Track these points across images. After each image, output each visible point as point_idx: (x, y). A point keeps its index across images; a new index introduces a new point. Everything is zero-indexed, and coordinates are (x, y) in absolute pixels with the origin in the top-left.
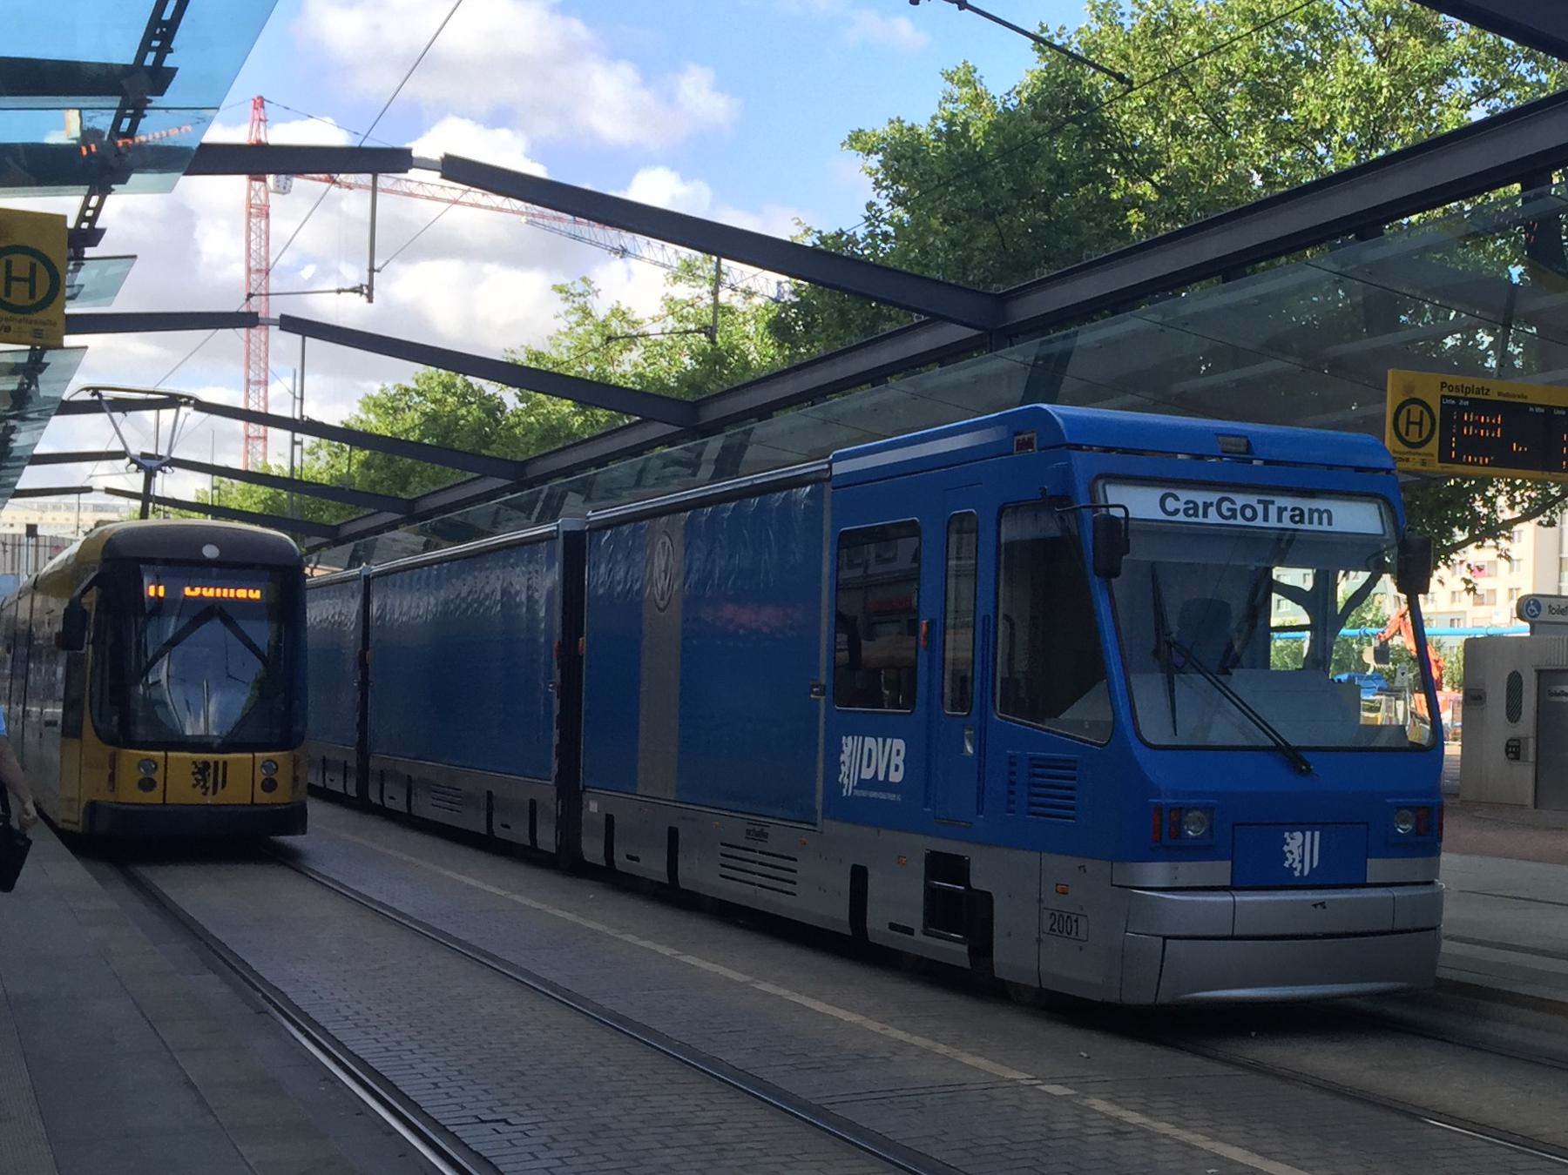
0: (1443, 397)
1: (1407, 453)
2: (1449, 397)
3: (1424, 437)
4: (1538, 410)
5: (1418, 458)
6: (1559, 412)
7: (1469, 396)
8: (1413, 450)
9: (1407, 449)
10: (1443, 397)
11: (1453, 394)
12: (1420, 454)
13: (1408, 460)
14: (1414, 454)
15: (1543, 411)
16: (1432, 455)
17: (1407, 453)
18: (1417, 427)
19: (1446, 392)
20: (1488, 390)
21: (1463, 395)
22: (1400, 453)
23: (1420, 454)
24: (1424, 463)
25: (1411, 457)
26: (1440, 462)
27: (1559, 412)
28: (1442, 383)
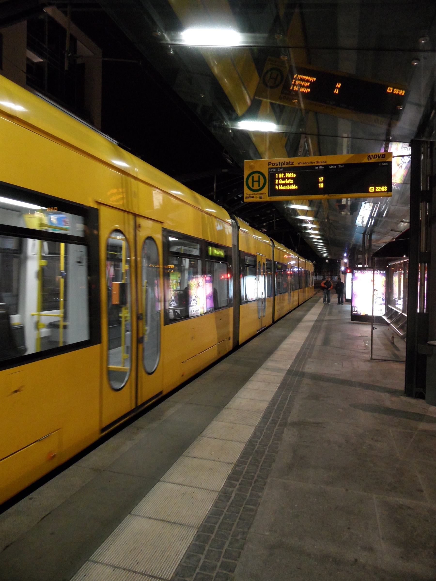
0: (269, 168)
1: (253, 194)
2: (272, 168)
3: (261, 186)
4: (320, 167)
5: (258, 196)
6: (332, 167)
7: (282, 166)
8: (255, 193)
9: (252, 193)
10: (269, 168)
11: (275, 166)
12: (259, 194)
13: (253, 197)
15: (323, 167)
16: (265, 194)
17: (253, 194)
18: (257, 183)
19: (271, 166)
20: (293, 162)
21: (280, 166)
22: (250, 194)
23: (259, 194)
24: (261, 197)
25: (255, 196)
26: (269, 196)
27: (332, 167)
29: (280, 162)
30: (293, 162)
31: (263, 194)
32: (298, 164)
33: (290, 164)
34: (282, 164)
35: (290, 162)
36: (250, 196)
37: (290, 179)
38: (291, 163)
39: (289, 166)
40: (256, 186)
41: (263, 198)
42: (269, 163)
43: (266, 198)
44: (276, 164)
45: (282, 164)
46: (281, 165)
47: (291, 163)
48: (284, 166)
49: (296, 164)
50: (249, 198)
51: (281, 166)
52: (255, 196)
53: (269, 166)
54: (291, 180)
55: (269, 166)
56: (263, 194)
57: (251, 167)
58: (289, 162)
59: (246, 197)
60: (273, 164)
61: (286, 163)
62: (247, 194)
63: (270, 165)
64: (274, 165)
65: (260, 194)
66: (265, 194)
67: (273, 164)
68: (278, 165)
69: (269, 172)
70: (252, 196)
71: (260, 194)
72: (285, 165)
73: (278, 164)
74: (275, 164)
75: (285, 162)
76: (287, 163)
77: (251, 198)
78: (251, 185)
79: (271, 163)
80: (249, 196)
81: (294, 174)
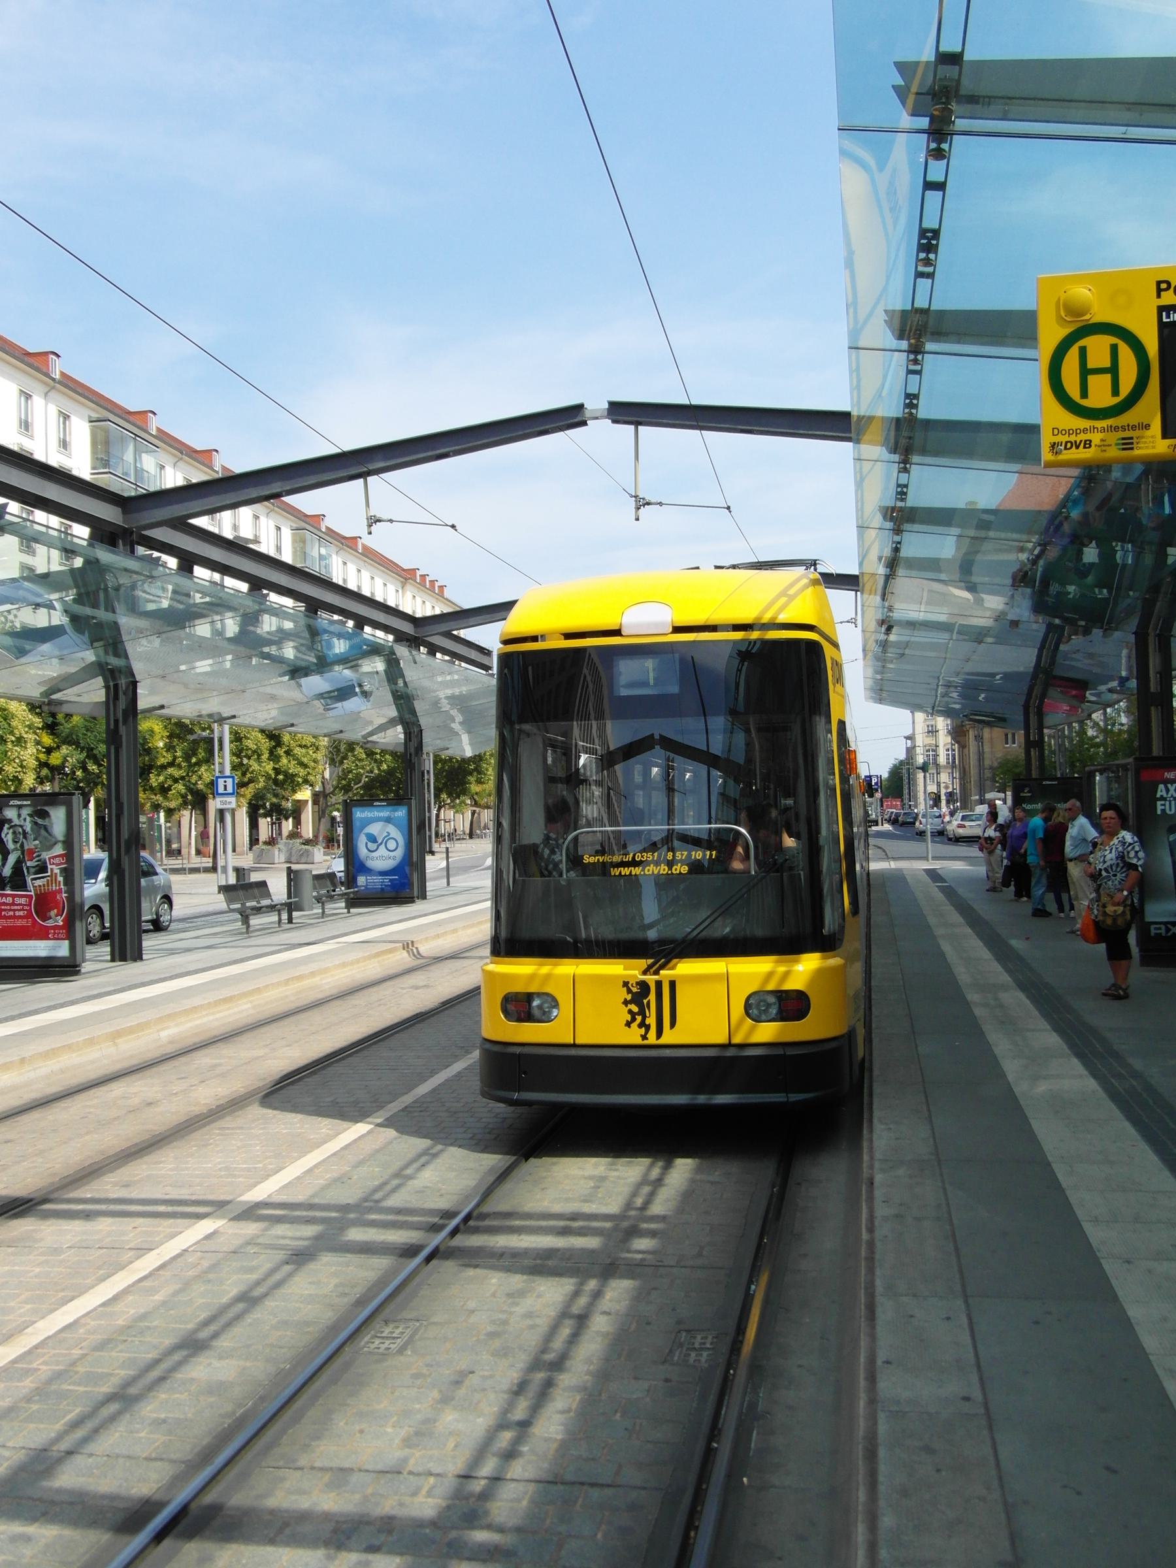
0: (1161, 309)
1: (1085, 431)
10: (1161, 309)
17: (1085, 431)
22: (1069, 432)
23: (1116, 429)
28: (1159, 283)
31: (1134, 428)
36: (1073, 438)
41: (1135, 446)
42: (1159, 283)
43: (1154, 447)
50: (1066, 448)
53: (1159, 296)
55: (1159, 296)
56: (1134, 428)
59: (1053, 445)
62: (1056, 431)
63: (1163, 293)
65: (1123, 428)
69: (1162, 326)
70: (1083, 437)
71: (1123, 428)
77: (1077, 447)
80: (1065, 438)
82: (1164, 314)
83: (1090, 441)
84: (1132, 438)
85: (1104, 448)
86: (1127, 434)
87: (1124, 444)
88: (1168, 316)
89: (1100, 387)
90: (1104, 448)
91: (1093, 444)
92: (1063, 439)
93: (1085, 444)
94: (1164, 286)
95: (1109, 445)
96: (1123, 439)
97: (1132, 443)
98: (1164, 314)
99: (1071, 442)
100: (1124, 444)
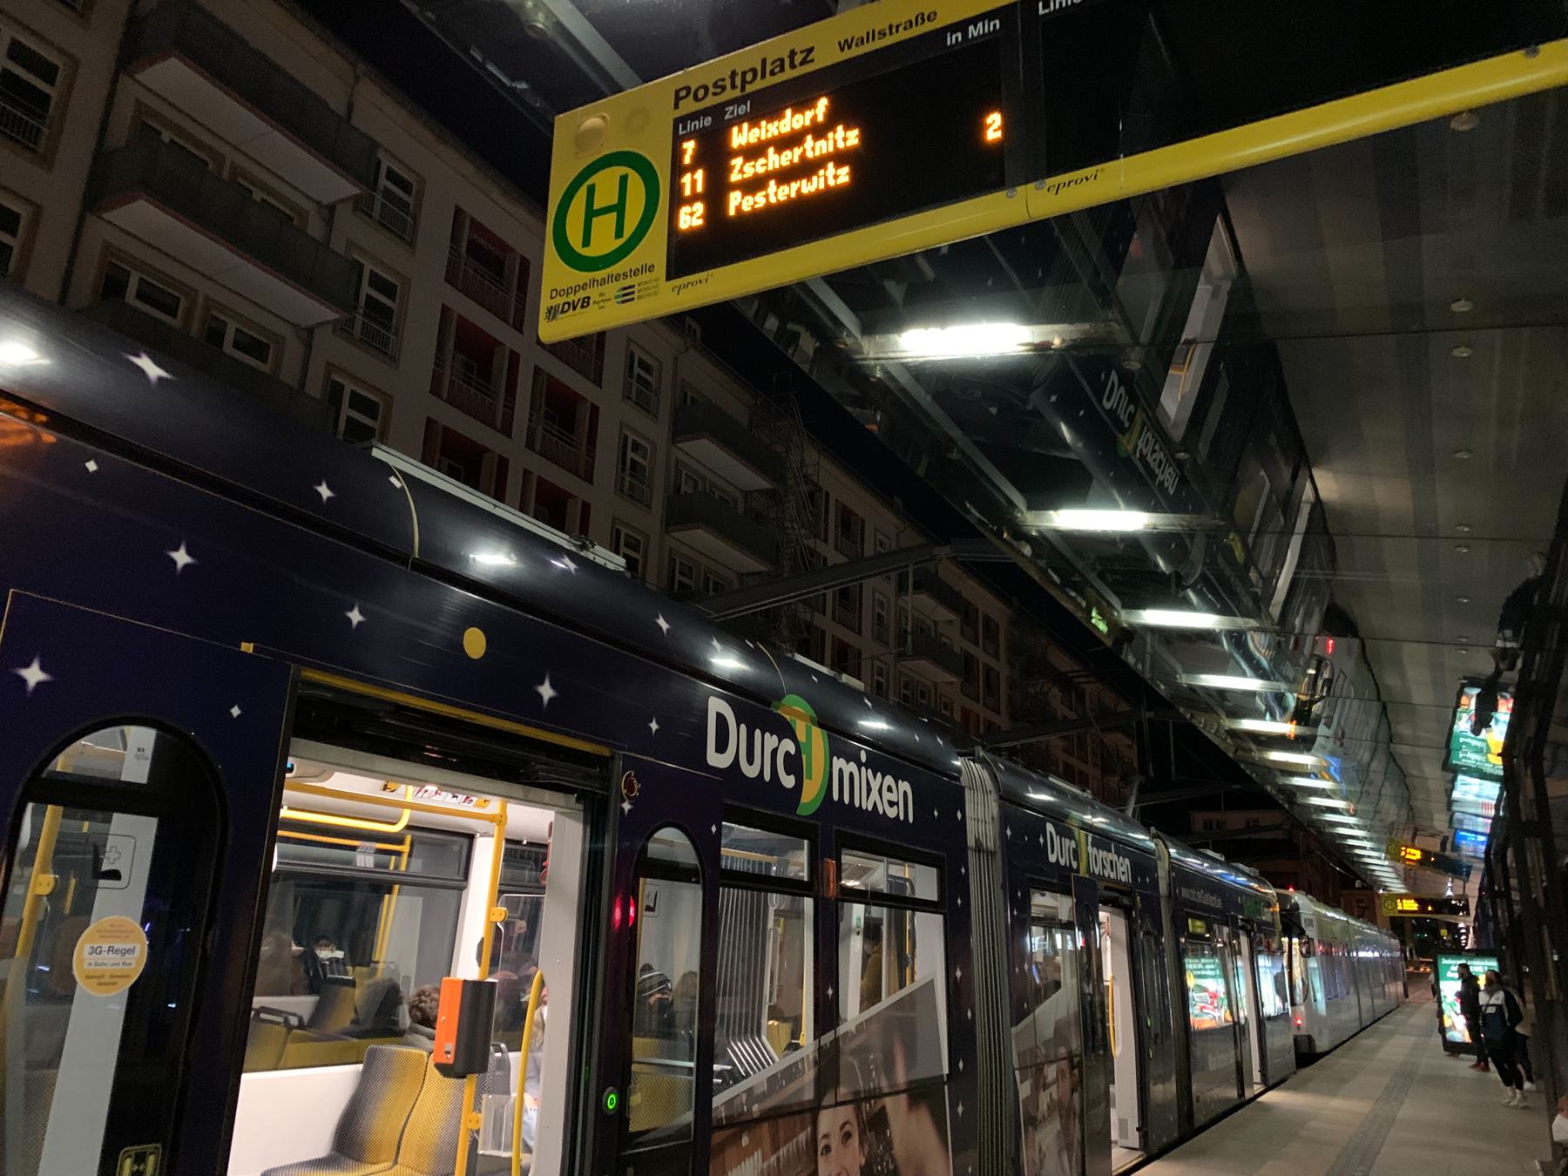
1: (584, 287)
5: (612, 289)
7: (749, 89)
8: (599, 275)
9: (586, 276)
11: (710, 101)
12: (617, 278)
13: (586, 302)
14: (604, 281)
16: (651, 268)
17: (584, 287)
19: (688, 106)
20: (810, 50)
21: (737, 93)
23: (617, 278)
25: (593, 293)
29: (739, 71)
30: (810, 50)
31: (636, 273)
32: (842, 49)
33: (793, 66)
34: (749, 77)
35: (792, 54)
36: (571, 298)
37: (831, 165)
38: (798, 59)
39: (789, 74)
40: (604, 240)
42: (677, 92)
44: (715, 85)
45: (749, 77)
46: (744, 83)
47: (798, 59)
48: (759, 84)
49: (827, 56)
50: (563, 312)
51: (743, 89)
52: (593, 293)
53: (676, 106)
54: (838, 165)
55: (676, 106)
56: (636, 273)
57: (583, 140)
58: (785, 55)
60: (701, 93)
61: (769, 68)
62: (556, 292)
64: (706, 95)
66: (651, 268)
67: (701, 93)
68: (724, 88)
70: (582, 294)
72: (763, 76)
73: (728, 83)
74: (712, 90)
75: (764, 61)
76: (773, 63)
77: (574, 309)
78: (574, 237)
79: (688, 89)
80: (565, 299)
81: (846, 129)
82: (681, 125)
83: (589, 298)
84: (633, 286)
85: (602, 304)
86: (627, 282)
87: (624, 295)
88: (684, 128)
89: (604, 227)
90: (602, 304)
91: (591, 302)
92: (560, 300)
93: (584, 302)
94: (683, 93)
95: (609, 300)
96: (624, 289)
97: (633, 293)
98: (681, 125)
99: (569, 303)
100: (624, 295)
